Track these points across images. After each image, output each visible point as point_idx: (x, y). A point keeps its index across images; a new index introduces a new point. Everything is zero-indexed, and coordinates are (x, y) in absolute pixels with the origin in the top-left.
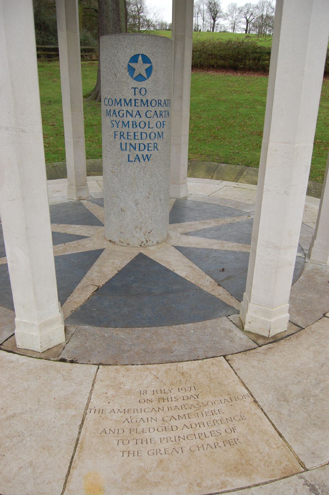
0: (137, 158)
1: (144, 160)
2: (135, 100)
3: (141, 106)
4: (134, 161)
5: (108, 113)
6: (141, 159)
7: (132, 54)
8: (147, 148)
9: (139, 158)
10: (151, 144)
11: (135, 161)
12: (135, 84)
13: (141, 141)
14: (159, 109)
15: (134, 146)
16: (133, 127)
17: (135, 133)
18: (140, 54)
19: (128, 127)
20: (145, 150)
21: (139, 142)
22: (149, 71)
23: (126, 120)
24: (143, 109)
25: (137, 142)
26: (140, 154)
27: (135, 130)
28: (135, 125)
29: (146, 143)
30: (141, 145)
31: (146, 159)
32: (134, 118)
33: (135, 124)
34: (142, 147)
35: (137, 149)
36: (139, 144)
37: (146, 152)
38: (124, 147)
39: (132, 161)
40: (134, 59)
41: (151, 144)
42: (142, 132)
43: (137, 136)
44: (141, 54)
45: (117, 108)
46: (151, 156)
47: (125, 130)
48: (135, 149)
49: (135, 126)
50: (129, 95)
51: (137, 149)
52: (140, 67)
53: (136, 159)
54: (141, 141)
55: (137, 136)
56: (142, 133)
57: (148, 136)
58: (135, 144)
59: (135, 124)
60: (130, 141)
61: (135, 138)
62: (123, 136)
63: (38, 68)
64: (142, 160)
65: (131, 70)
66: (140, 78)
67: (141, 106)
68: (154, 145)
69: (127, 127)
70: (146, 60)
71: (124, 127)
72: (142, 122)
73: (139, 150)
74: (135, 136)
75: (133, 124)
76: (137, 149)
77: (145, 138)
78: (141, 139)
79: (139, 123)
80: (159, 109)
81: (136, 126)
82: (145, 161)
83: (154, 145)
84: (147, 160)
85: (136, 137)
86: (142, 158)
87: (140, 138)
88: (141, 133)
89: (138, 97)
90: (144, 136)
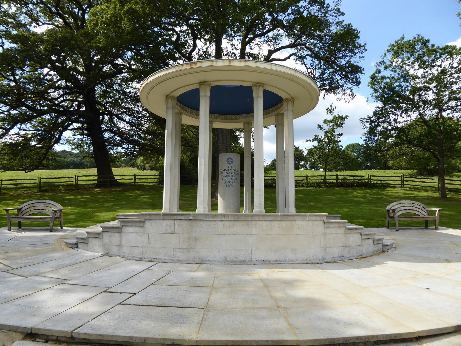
5: (221, 174)
12: (228, 165)
14: (235, 172)
22: (232, 162)
23: (226, 175)
24: (231, 172)
40: (228, 159)
45: (223, 172)
47: (226, 178)
50: (227, 168)
52: (230, 161)
63: (181, 184)
65: (228, 162)
66: (230, 164)
70: (231, 159)
80: (235, 172)
89: (230, 169)
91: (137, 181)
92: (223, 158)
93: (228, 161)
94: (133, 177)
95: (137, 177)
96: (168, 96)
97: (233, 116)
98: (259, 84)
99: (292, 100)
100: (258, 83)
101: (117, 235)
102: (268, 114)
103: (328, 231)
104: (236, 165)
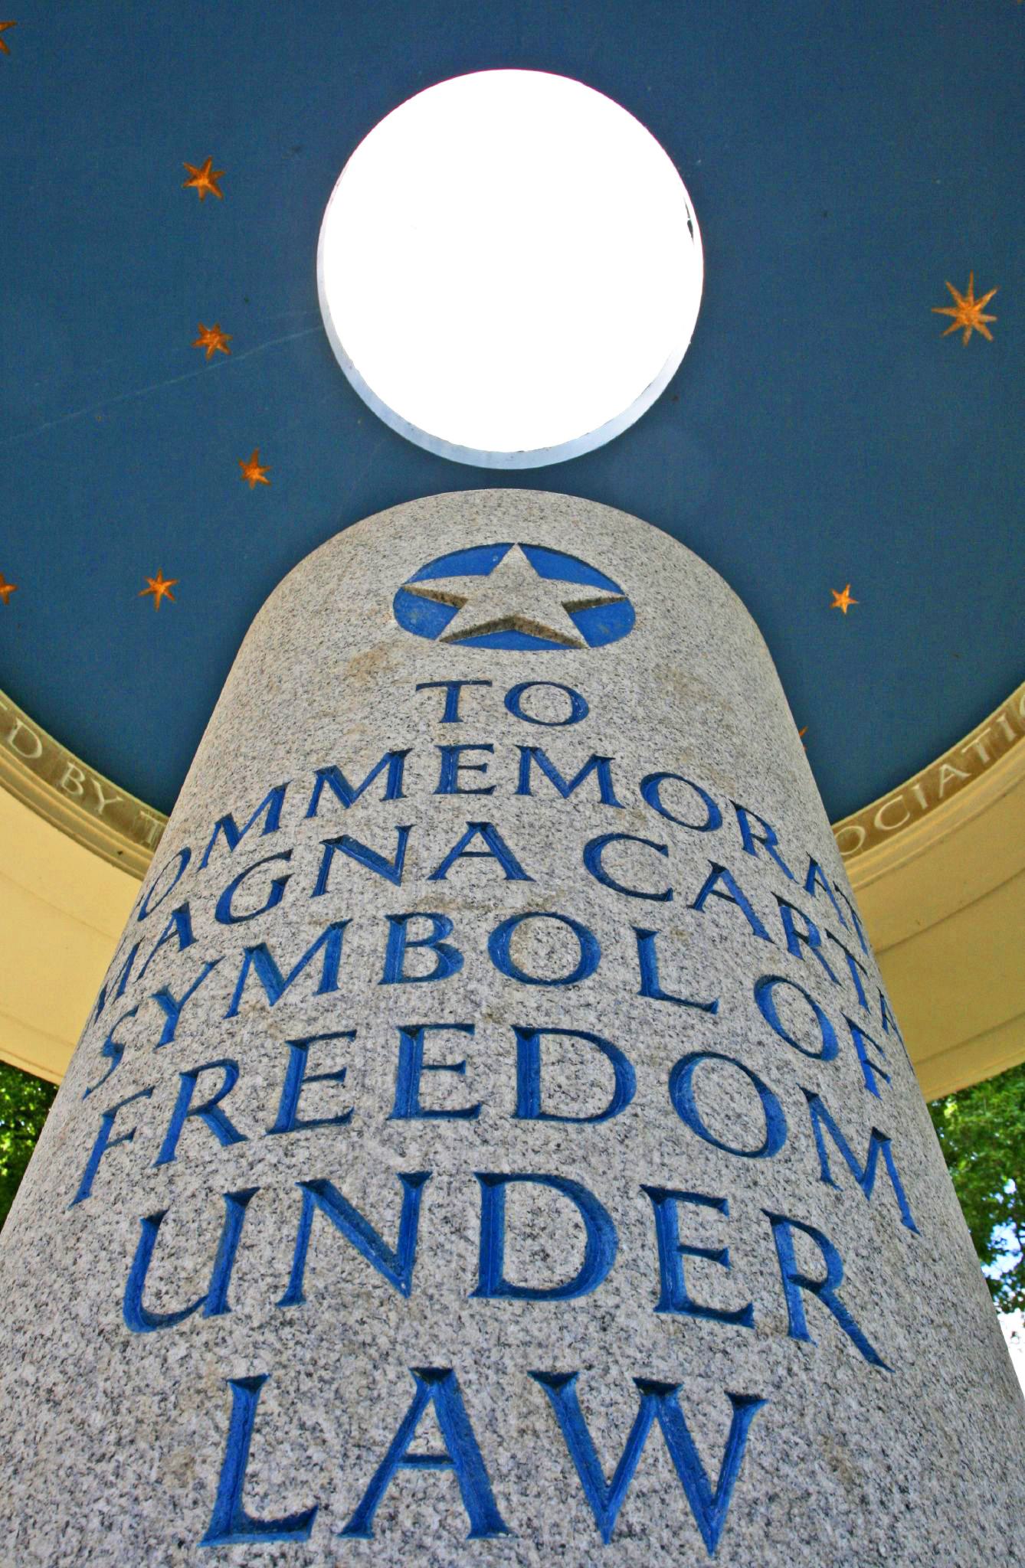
0: (428, 1438)
1: (604, 1494)
2: (450, 754)
3: (524, 789)
4: (343, 1504)
6: (525, 1473)
7: (443, 548)
8: (637, 1251)
9: (463, 1456)
10: (718, 1204)
11: (359, 1525)
13: (532, 1146)
15: (387, 1223)
16: (393, 974)
17: (412, 1034)
18: (510, 545)
19: (318, 978)
20: (601, 1294)
21: (482, 1159)
25: (452, 1153)
26: (499, 1356)
27: (414, 1003)
28: (421, 945)
29: (627, 1163)
30: (517, 1200)
31: (637, 1484)
32: (426, 889)
33: (433, 941)
34: (545, 1239)
35: (428, 1268)
36: (492, 1182)
37: (625, 1334)
38: (182, 1269)
39: (299, 1524)
41: (718, 1204)
42: (540, 1021)
43: (459, 1068)
44: (521, 545)
46: (753, 1439)
48: (399, 1264)
49: (425, 961)
51: (447, 1259)
53: (397, 1456)
54: (532, 1146)
55: (446, 1078)
56: (546, 1042)
57: (651, 1086)
58: (414, 1182)
59: (433, 941)
60: (313, 1155)
61: (407, 1105)
62: (209, 1109)
64: (539, 1491)
67: (524, 789)
68: (785, 1257)
69: (301, 993)
71: (255, 994)
72: (537, 923)
73: (490, 1282)
74: (411, 1067)
75: (396, 947)
76: (447, 1259)
77: (601, 1100)
78: (528, 1106)
79: (489, 925)
81: (449, 962)
82: (632, 1512)
83: (785, 1257)
84: (679, 1504)
85: (434, 1089)
86: (554, 1465)
87: (509, 1099)
88: (527, 1036)
90: (574, 1077)
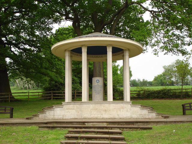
22: (99, 82)
40: (97, 80)
52: (98, 81)
91: (30, 97)
92: (95, 79)
93: (98, 81)
94: (27, 94)
95: (30, 94)
96: (65, 50)
97: (100, 56)
98: (110, 45)
99: (129, 50)
100: (109, 45)
101: (52, 111)
102: (119, 54)
103: (132, 108)
104: (101, 83)
